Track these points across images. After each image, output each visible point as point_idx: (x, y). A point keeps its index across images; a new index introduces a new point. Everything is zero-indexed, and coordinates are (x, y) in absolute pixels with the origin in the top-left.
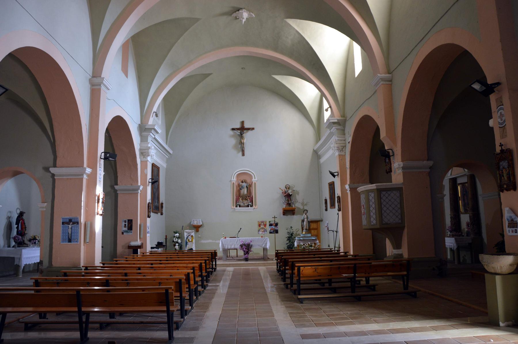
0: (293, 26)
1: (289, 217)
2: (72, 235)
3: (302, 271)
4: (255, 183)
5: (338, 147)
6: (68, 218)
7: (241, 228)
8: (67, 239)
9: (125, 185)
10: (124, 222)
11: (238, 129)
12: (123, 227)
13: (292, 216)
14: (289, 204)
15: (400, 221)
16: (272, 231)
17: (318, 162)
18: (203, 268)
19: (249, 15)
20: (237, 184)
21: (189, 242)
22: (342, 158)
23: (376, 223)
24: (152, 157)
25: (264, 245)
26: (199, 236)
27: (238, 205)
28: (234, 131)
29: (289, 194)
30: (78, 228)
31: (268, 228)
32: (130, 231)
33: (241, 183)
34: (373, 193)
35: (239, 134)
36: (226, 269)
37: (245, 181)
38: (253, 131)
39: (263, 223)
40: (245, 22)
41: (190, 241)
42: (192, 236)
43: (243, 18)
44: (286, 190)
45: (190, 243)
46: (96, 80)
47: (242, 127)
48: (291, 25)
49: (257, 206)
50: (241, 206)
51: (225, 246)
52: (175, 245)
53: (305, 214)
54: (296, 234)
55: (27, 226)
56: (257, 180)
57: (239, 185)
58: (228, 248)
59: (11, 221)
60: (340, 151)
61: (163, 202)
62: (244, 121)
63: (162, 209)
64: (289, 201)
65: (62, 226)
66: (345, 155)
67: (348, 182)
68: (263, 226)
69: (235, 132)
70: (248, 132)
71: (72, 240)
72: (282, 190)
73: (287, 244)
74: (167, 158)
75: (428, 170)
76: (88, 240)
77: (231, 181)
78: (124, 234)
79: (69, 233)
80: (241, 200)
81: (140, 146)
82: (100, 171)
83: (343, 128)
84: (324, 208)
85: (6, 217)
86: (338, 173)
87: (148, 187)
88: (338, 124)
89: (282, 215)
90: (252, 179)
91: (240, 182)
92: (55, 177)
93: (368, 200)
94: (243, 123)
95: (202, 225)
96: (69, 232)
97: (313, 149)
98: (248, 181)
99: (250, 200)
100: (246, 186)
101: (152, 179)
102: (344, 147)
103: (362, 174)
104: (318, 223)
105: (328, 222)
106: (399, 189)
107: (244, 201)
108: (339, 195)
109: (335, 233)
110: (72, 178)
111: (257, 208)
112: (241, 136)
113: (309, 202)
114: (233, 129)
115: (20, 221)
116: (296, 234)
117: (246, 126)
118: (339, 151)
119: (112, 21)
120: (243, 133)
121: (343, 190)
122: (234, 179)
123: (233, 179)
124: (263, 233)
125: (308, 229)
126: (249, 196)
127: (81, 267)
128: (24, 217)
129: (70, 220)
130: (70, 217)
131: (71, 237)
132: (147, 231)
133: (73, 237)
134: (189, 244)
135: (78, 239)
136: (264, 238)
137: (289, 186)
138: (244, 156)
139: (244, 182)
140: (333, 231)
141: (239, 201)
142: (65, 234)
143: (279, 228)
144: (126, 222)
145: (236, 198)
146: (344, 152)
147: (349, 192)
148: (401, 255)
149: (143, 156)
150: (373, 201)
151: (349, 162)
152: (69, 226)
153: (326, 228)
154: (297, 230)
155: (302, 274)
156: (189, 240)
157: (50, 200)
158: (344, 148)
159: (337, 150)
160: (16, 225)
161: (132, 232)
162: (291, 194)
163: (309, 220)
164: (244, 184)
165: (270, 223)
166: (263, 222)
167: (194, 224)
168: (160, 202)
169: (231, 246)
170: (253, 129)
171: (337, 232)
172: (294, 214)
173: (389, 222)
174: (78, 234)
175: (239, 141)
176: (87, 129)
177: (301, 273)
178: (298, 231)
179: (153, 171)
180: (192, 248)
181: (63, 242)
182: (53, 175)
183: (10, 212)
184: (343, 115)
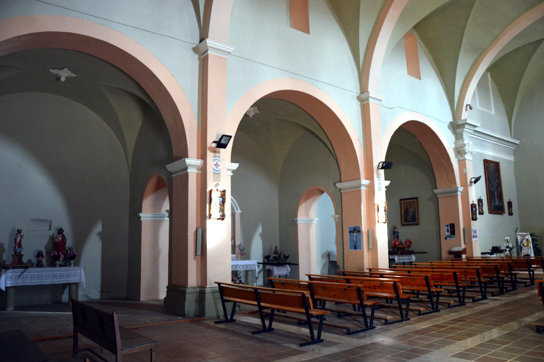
6: (353, 227)
8: (353, 247)
9: (444, 188)
18: (458, 277)
21: (525, 246)
24: (472, 154)
41: (526, 245)
42: (527, 240)
45: (525, 247)
46: (364, 96)
74: (513, 149)
76: (371, 248)
78: (448, 239)
129: (355, 229)
131: (356, 245)
132: (472, 236)
133: (357, 245)
134: (525, 249)
142: (351, 242)
149: (460, 155)
161: (454, 237)
176: (361, 143)
180: (529, 253)
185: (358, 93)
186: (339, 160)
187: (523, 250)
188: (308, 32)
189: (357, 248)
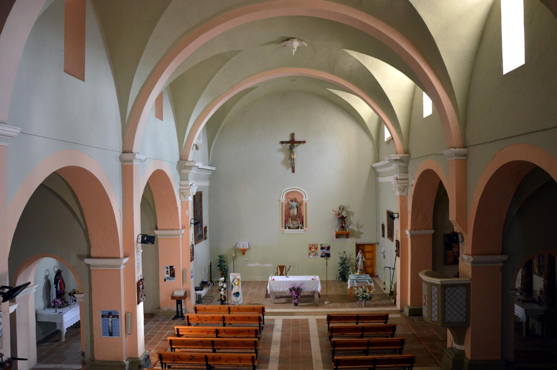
1: (342, 240)
2: (113, 328)
6: (107, 311)
7: (290, 266)
8: (108, 333)
11: (287, 142)
13: (346, 239)
14: (343, 228)
15: (465, 320)
16: (323, 255)
17: (376, 181)
19: (299, 44)
20: (286, 203)
22: (403, 200)
26: (246, 259)
27: (287, 226)
28: (284, 145)
29: (343, 216)
30: (118, 322)
31: (320, 252)
32: (172, 277)
33: (291, 202)
35: (289, 147)
36: (273, 320)
37: (295, 200)
39: (314, 246)
40: (295, 52)
41: (237, 284)
43: (294, 49)
44: (339, 211)
45: (236, 286)
47: (291, 140)
49: (307, 228)
51: (273, 288)
52: (220, 290)
54: (350, 258)
55: (65, 284)
56: (308, 200)
57: (288, 204)
59: (49, 279)
60: (402, 192)
61: (206, 226)
63: (206, 233)
64: (343, 224)
65: (102, 320)
66: (407, 195)
68: (314, 249)
69: (283, 146)
70: (298, 145)
71: (113, 333)
72: (336, 212)
73: (339, 270)
75: (502, 264)
77: (279, 200)
78: (167, 281)
79: (110, 327)
80: (291, 221)
81: (181, 185)
82: (138, 263)
83: (406, 165)
84: (381, 233)
85: (44, 277)
86: (398, 215)
87: (190, 230)
89: (335, 238)
90: (303, 198)
91: (289, 200)
92: (91, 268)
93: (430, 294)
94: (293, 135)
95: (248, 248)
96: (110, 326)
97: (370, 165)
98: (299, 200)
99: (299, 219)
101: (195, 219)
102: (406, 187)
103: (425, 219)
105: (384, 250)
106: (467, 286)
107: (294, 222)
108: (398, 239)
109: (392, 270)
110: (109, 269)
111: (307, 231)
112: (291, 149)
113: (364, 224)
115: (58, 280)
116: (350, 258)
117: (297, 139)
118: (401, 191)
120: (293, 148)
121: (403, 234)
122: (283, 199)
123: (282, 198)
124: (314, 257)
125: (362, 269)
126: (299, 217)
127: (123, 362)
128: (63, 274)
129: (110, 314)
131: (112, 331)
133: (114, 331)
134: (235, 288)
137: (343, 207)
138: (294, 172)
141: (289, 222)
142: (105, 328)
143: (331, 252)
144: (168, 269)
145: (285, 219)
146: (406, 192)
147: (409, 237)
148: (463, 352)
149: (183, 196)
150: (436, 296)
151: (411, 207)
152: (109, 320)
153: (383, 254)
154: (350, 255)
157: (87, 290)
158: (405, 188)
159: (399, 190)
160: (54, 284)
161: (174, 279)
162: (345, 216)
164: (294, 204)
165: (322, 246)
166: (314, 245)
167: (240, 248)
168: (204, 227)
169: (280, 288)
170: (304, 142)
171: (394, 269)
172: (347, 237)
178: (351, 255)
179: (195, 200)
180: (239, 291)
182: (89, 266)
183: (48, 270)
184: (407, 152)
185: (121, 152)
186: (90, 231)
188: (82, 77)
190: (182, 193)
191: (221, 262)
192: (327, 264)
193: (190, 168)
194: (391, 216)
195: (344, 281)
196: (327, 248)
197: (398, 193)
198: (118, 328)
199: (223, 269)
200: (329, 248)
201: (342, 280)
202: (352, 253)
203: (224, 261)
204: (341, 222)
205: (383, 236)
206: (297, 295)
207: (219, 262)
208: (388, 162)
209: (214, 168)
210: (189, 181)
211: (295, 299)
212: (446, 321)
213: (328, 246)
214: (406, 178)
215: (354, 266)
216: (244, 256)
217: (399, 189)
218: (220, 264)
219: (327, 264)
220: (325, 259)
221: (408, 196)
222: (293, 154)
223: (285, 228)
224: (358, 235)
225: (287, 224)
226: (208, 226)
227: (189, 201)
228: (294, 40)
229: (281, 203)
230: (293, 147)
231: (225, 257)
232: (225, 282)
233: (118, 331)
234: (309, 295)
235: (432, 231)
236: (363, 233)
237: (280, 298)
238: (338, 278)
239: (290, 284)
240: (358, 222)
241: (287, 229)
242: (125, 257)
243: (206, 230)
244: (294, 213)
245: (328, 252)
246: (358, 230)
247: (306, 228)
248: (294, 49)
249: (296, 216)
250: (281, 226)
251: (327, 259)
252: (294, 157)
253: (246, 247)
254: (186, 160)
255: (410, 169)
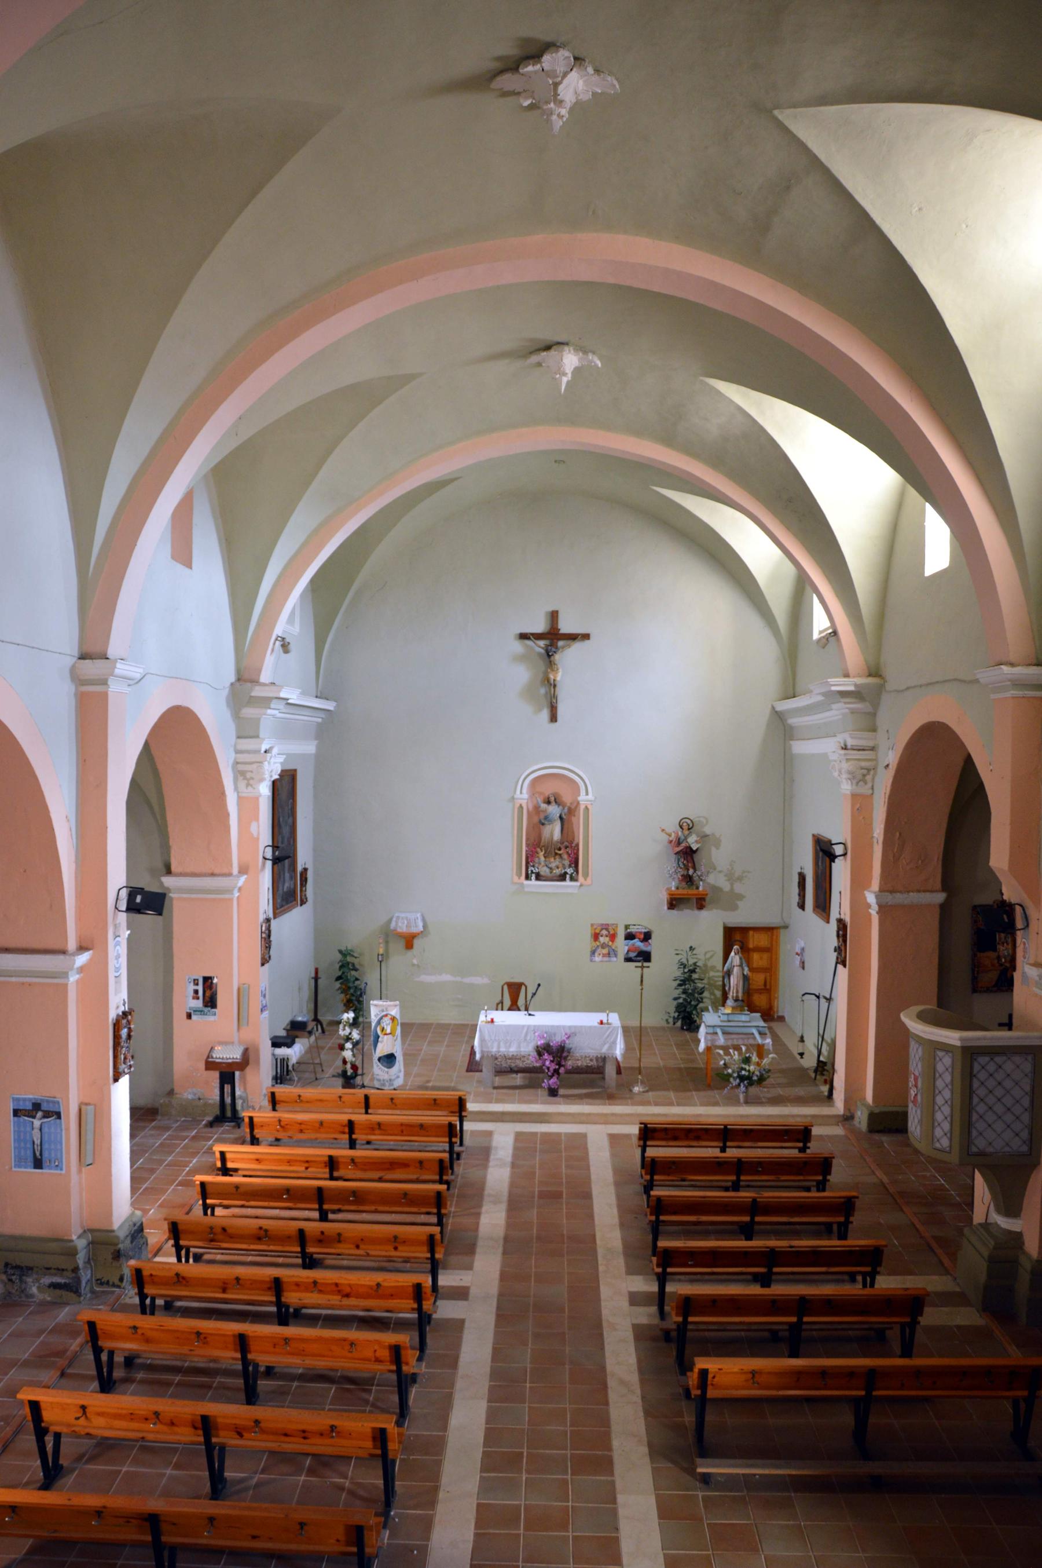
0: (727, 395)
1: (686, 916)
3: (714, 1377)
4: (586, 807)
5: (849, 772)
6: (30, 1100)
7: (539, 985)
8: (30, 1159)
10: (192, 983)
11: (538, 637)
12: (191, 998)
13: (696, 912)
14: (688, 880)
15: (1025, 1149)
16: (632, 955)
18: (425, 1293)
19: (580, 360)
20: (531, 808)
21: (386, 1034)
22: (860, 805)
23: (950, 1146)
25: (606, 1047)
26: (415, 962)
27: (532, 871)
28: (528, 642)
30: (59, 1131)
31: (622, 946)
32: (209, 1009)
33: (544, 806)
34: (950, 1055)
35: (542, 651)
36: (490, 1134)
37: (555, 799)
38: (587, 643)
39: (607, 929)
40: (568, 382)
41: (388, 1031)
43: (565, 374)
44: (680, 833)
45: (386, 1036)
48: (720, 393)
50: (542, 876)
51: (489, 1044)
52: (342, 1048)
53: (735, 954)
54: (705, 965)
57: (537, 808)
58: (499, 1052)
61: (306, 866)
62: (557, 612)
64: (688, 870)
65: (14, 1122)
66: (872, 794)
67: (875, 885)
68: (607, 939)
70: (569, 646)
72: (670, 835)
73: (675, 999)
77: (513, 799)
78: (194, 1017)
79: (36, 1142)
80: (542, 859)
81: (237, 752)
82: (117, 966)
83: (870, 709)
84: (796, 899)
86: (846, 848)
88: (856, 698)
89: (666, 907)
90: (579, 795)
91: (540, 800)
93: (932, 1074)
94: (554, 616)
95: (422, 932)
97: (770, 707)
98: (567, 799)
99: (569, 855)
100: (558, 815)
101: (275, 847)
102: (869, 770)
103: (920, 861)
104: (772, 935)
105: (803, 945)
108: (842, 917)
109: (824, 1004)
111: (589, 885)
112: (549, 655)
113: (749, 872)
114: (523, 636)
116: (705, 965)
117: (566, 626)
118: (854, 782)
119: (133, 467)
120: (555, 652)
121: (857, 904)
122: (523, 796)
123: (521, 793)
125: (740, 999)
126: (566, 847)
127: (72, 1241)
129: (37, 1106)
130: (36, 1097)
131: (41, 1154)
133: (46, 1154)
135: (62, 1162)
136: (609, 1028)
137: (689, 822)
138: (556, 721)
139: (554, 803)
140: (816, 996)
141: (536, 860)
142: (22, 1145)
143: (654, 947)
144: (197, 984)
145: (526, 851)
146: (870, 785)
147: (874, 911)
149: (246, 781)
150: (948, 1078)
151: (882, 826)
152: (33, 1123)
153: (798, 958)
154: (708, 956)
155: (712, 1385)
156: (383, 1028)
158: (868, 773)
159: (849, 779)
162: (694, 849)
163: (745, 973)
164: (554, 810)
165: (628, 930)
166: (606, 927)
167: (399, 930)
169: (510, 1046)
170: (586, 637)
171: (829, 1000)
173: (991, 1150)
174: (62, 1153)
175: (541, 676)
176: (71, 830)
177: (709, 1383)
178: (711, 957)
180: (394, 1052)
181: (19, 1166)
184: (875, 672)
185: (74, 656)
187: (381, 1042)
189: (45, 1164)
190: (240, 773)
191: (345, 970)
192: (642, 981)
193: (265, 702)
194: (825, 852)
195: (687, 1030)
196: (642, 936)
197: (847, 787)
198: (59, 1147)
199: (349, 988)
200: (647, 937)
201: (682, 1028)
202: (712, 951)
203: (353, 965)
204: (684, 864)
205: (802, 906)
206: (557, 1064)
207: (341, 967)
208: (820, 698)
209: (330, 706)
210: (264, 739)
211: (551, 1077)
212: (974, 1149)
213: (646, 931)
214: (871, 744)
215: (718, 989)
216: (410, 953)
217: (850, 776)
218: (343, 973)
219: (642, 981)
220: (636, 967)
221: (876, 797)
222: (553, 670)
223: (527, 877)
224: (732, 901)
225: (533, 866)
226: (310, 866)
227: (260, 796)
228: (566, 348)
229: (518, 805)
230: (554, 650)
231: (355, 955)
232: (355, 1024)
233: (59, 1156)
234: (591, 1066)
235: (940, 897)
236: (744, 897)
237: (508, 1072)
238: (671, 1020)
239: (536, 1034)
240: (731, 865)
241: (531, 880)
242: (82, 949)
243: (306, 879)
244: (552, 835)
245: (647, 947)
246: (732, 889)
247: (585, 880)
248: (565, 374)
249: (559, 845)
250: (515, 871)
251: (642, 967)
252: (555, 677)
253: (416, 926)
254: (255, 682)
255: (883, 719)
